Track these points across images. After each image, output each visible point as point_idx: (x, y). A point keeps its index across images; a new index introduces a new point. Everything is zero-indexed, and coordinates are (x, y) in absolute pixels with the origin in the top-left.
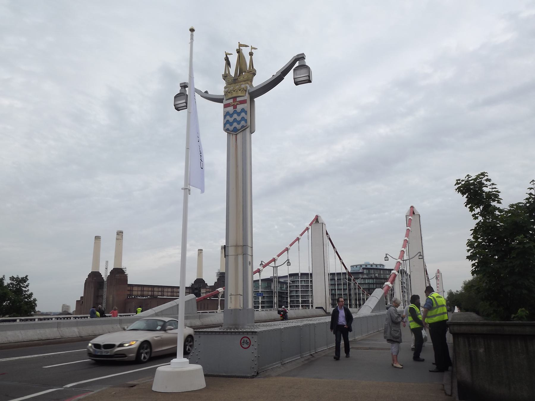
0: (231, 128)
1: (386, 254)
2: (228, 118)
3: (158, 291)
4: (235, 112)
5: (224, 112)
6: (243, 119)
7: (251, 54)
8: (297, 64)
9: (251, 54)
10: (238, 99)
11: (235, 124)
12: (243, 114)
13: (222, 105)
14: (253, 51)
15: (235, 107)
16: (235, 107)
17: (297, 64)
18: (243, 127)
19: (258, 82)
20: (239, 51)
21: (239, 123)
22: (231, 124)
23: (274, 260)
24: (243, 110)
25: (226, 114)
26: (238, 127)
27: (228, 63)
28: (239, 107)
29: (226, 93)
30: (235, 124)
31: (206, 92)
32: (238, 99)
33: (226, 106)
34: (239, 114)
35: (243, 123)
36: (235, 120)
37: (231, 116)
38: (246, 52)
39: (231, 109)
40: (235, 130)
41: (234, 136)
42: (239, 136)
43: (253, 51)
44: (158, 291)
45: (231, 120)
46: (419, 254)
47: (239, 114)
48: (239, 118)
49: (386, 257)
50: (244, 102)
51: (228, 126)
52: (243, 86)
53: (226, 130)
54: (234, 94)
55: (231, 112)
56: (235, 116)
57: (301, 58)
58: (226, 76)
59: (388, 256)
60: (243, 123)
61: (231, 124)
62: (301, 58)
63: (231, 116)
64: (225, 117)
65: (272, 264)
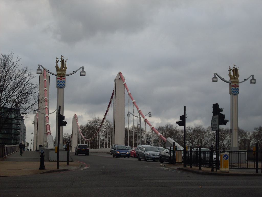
0: (60, 87)
9: (66, 61)
10: (62, 77)
12: (64, 83)
16: (61, 80)
18: (64, 87)
21: (62, 85)
26: (62, 87)
28: (63, 80)
31: (49, 70)
34: (62, 82)
36: (61, 84)
39: (59, 80)
45: (60, 84)
47: (62, 82)
48: (62, 84)
54: (61, 76)
56: (61, 83)
58: (57, 67)
60: (64, 86)
63: (60, 82)
64: (57, 82)
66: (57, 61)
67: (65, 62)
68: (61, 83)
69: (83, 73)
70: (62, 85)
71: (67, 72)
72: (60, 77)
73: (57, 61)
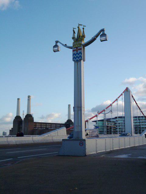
0: (76, 60)
2: (74, 56)
3: (49, 126)
4: (77, 53)
5: (73, 53)
6: (80, 56)
7: (83, 29)
8: (101, 33)
9: (83, 29)
10: (78, 48)
11: (77, 59)
12: (80, 54)
13: (72, 50)
14: (84, 27)
15: (77, 51)
16: (77, 51)
17: (101, 33)
18: (80, 59)
19: (86, 40)
20: (78, 28)
21: (79, 58)
22: (76, 58)
23: (104, 110)
25: (74, 54)
26: (78, 59)
27: (74, 32)
28: (79, 51)
29: (73, 45)
30: (77, 59)
31: (66, 45)
32: (78, 48)
33: (73, 51)
34: (79, 54)
35: (80, 58)
36: (77, 57)
37: (76, 55)
38: (81, 27)
39: (75, 52)
40: (77, 61)
41: (77, 63)
42: (79, 63)
43: (84, 27)
44: (49, 126)
45: (76, 57)
47: (79, 54)
48: (78, 56)
50: (81, 49)
51: (74, 59)
52: (80, 42)
53: (74, 61)
54: (77, 46)
55: (75, 53)
56: (77, 55)
57: (103, 30)
58: (73, 38)
60: (80, 58)
61: (76, 58)
62: (103, 30)
63: (76, 55)
65: (103, 112)
67: (82, 30)
68: (77, 55)
70: (79, 58)
72: (75, 49)
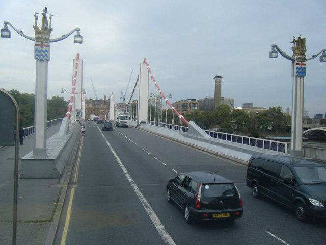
1: (6, 24)
9: (50, 18)
10: (44, 44)
12: (46, 53)
21: (44, 57)
24: (46, 50)
25: (36, 50)
26: (44, 59)
33: (36, 45)
36: (42, 55)
37: (39, 52)
39: (39, 48)
45: (40, 54)
46: (76, 33)
49: (5, 29)
51: (37, 56)
54: (42, 41)
56: (42, 52)
58: (36, 27)
59: (9, 27)
61: (39, 56)
62: (78, 30)
63: (39, 52)
64: (35, 51)
66: (37, 17)
67: (49, 20)
68: (42, 52)
69: (78, 39)
71: (53, 35)
73: (37, 17)
